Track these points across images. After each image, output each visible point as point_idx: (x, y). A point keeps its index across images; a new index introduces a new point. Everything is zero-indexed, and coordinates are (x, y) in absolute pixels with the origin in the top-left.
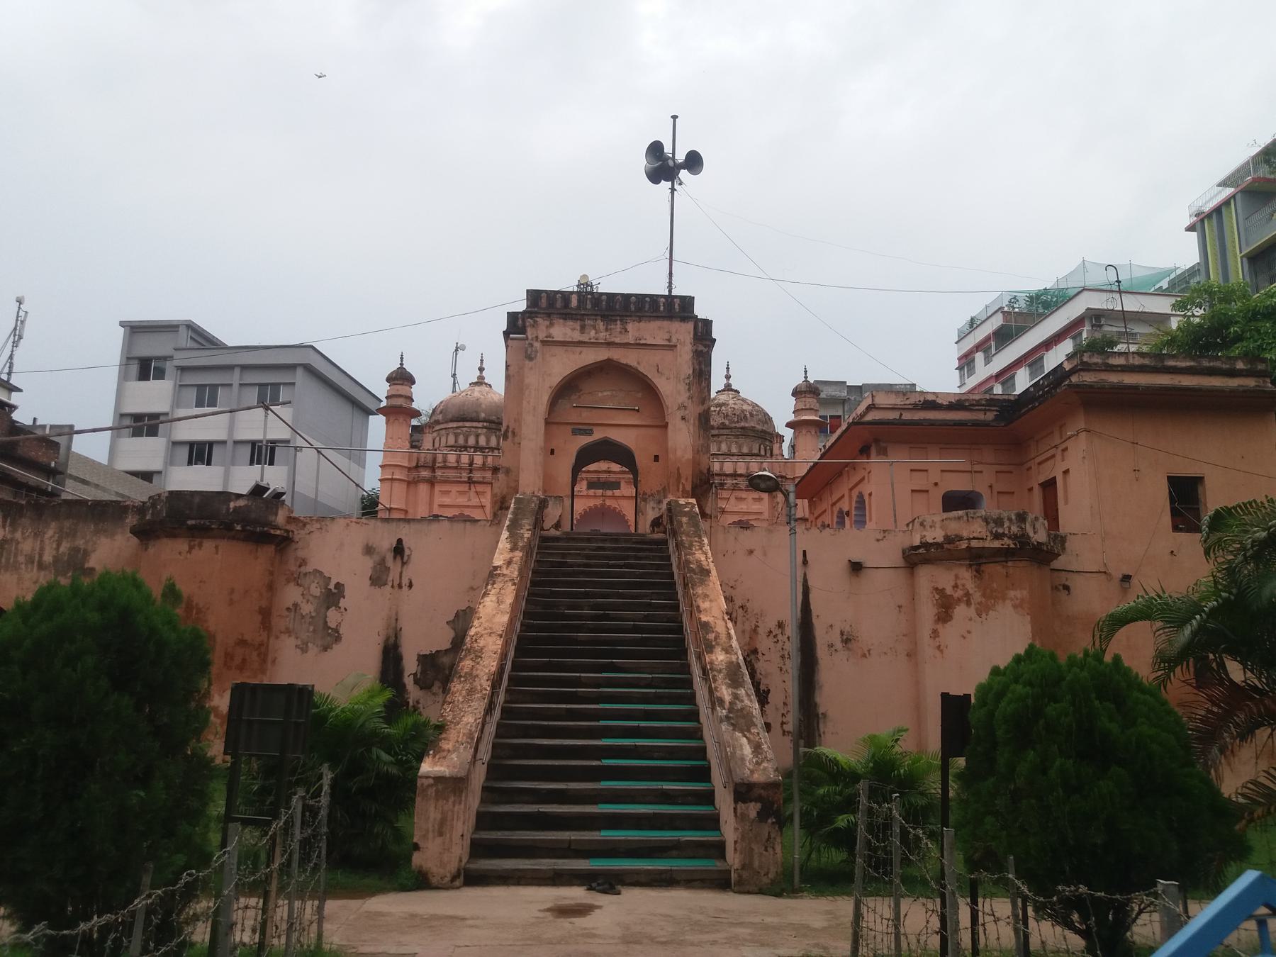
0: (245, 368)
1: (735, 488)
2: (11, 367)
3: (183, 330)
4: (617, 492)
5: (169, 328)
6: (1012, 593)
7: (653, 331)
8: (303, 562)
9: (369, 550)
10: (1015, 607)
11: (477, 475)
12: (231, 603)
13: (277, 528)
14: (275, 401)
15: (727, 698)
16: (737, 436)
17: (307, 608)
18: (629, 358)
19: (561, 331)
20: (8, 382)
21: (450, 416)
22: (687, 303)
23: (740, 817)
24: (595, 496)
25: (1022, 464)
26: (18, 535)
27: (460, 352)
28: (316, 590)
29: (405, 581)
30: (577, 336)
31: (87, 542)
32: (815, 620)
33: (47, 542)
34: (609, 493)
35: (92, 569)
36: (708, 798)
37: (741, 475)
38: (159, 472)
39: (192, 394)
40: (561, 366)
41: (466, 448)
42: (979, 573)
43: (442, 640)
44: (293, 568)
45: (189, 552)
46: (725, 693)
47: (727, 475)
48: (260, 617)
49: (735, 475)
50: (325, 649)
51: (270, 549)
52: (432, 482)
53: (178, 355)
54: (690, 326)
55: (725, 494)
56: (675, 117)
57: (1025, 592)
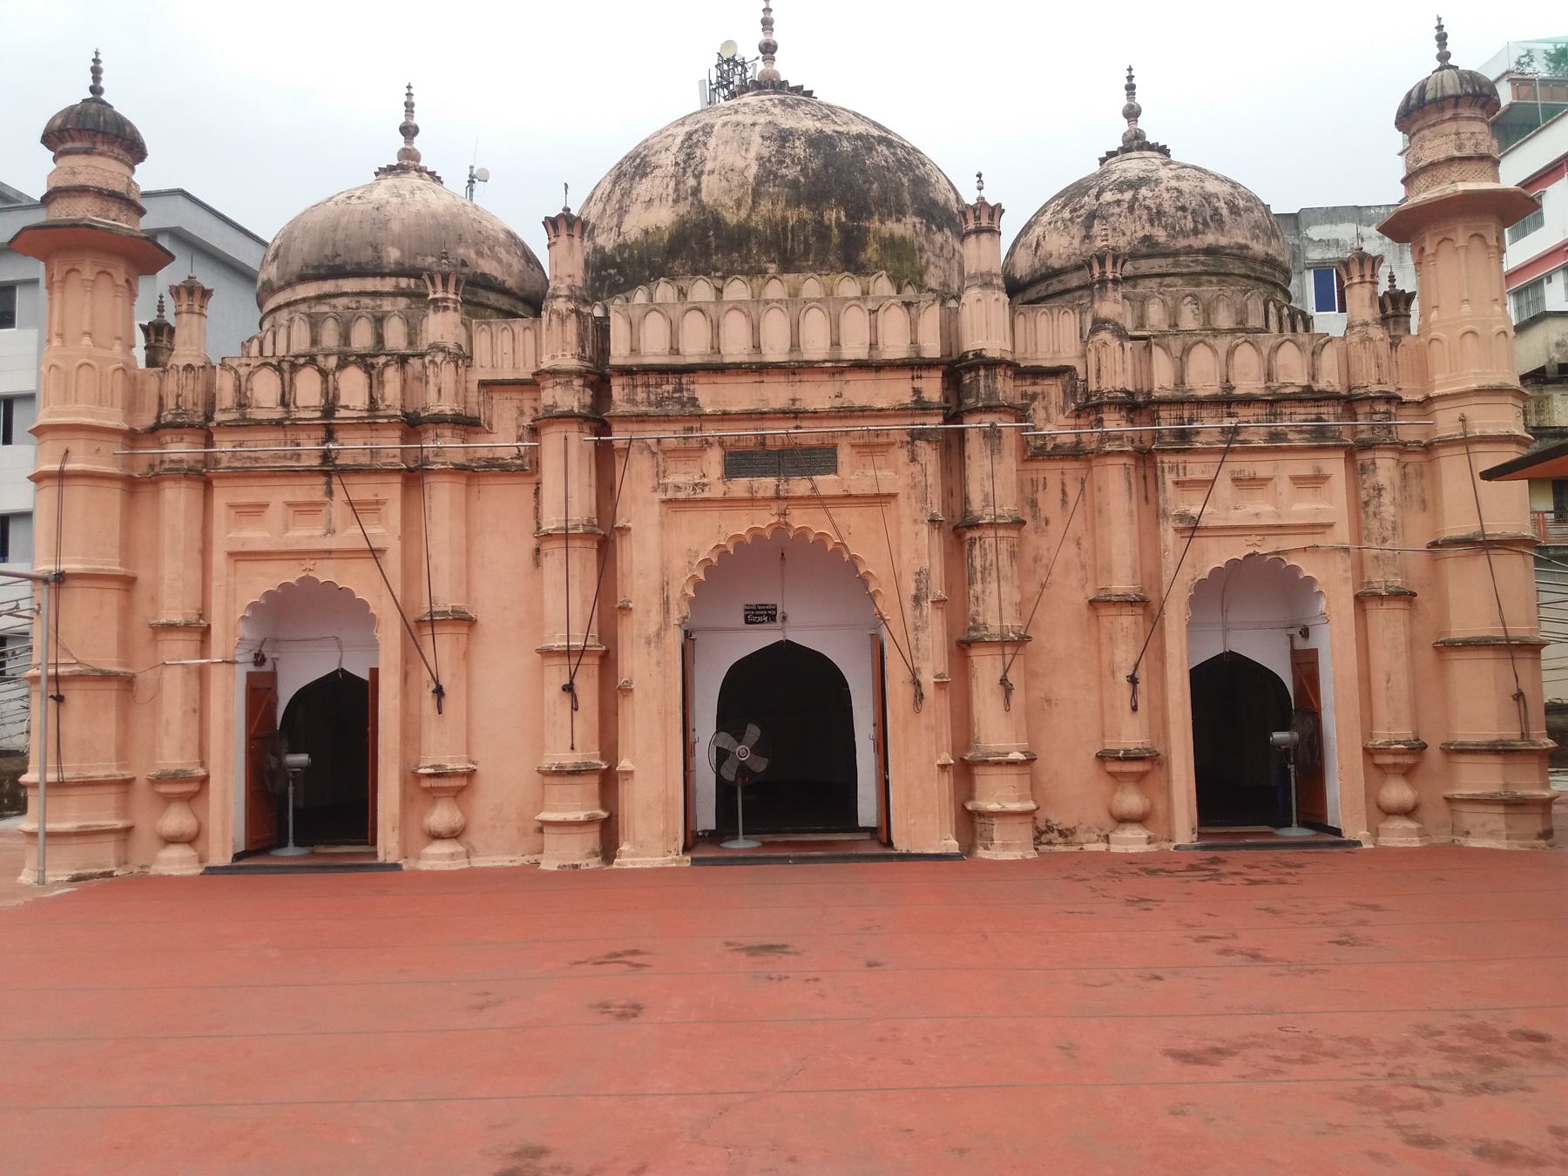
1: (1232, 443)
4: (827, 484)
11: (351, 447)
16: (1194, 277)
21: (295, 266)
24: (752, 501)
27: (478, 185)
34: (800, 486)
37: (1248, 400)
47: (1200, 403)
49: (1226, 401)
52: (202, 477)
55: (1197, 468)
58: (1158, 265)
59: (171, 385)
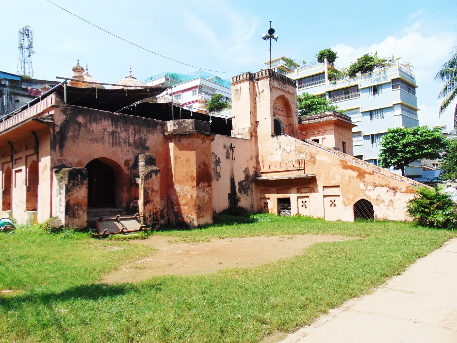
9: (225, 147)
18: (286, 95)
26: (119, 130)
29: (234, 158)
30: (278, 86)
31: (145, 136)
33: (130, 134)
35: (148, 147)
45: (202, 144)
50: (218, 180)
56: (270, 22)
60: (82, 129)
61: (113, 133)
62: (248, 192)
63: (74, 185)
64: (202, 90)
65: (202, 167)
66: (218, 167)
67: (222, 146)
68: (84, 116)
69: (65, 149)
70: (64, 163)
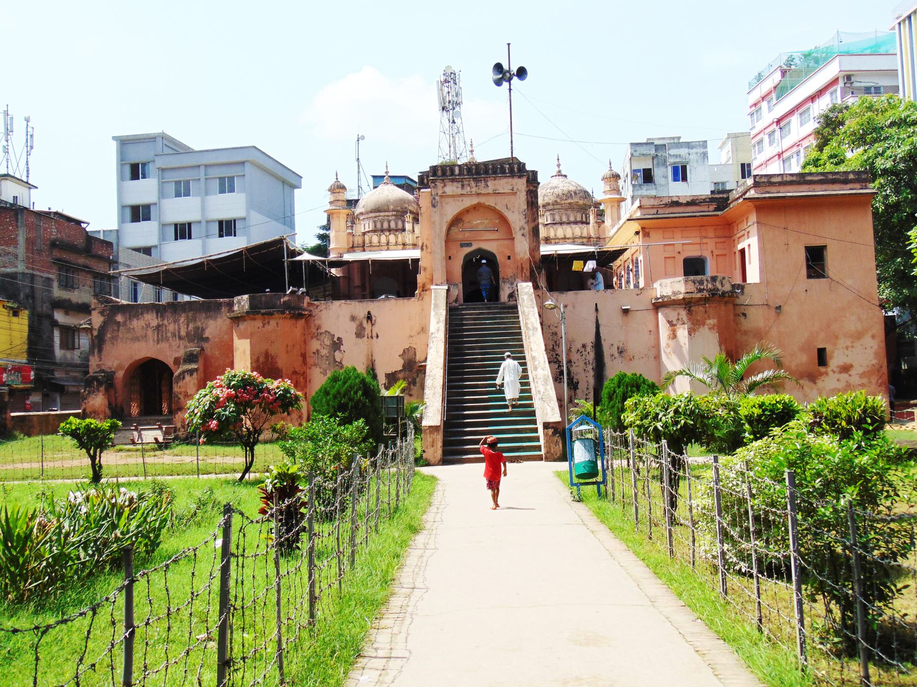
0: (206, 166)
2: (28, 171)
3: (159, 140)
5: (151, 139)
6: (708, 322)
7: (503, 184)
8: (319, 328)
9: (353, 318)
10: (710, 329)
12: (287, 352)
13: (304, 310)
14: (232, 190)
15: (542, 390)
16: (566, 209)
17: (324, 352)
18: (490, 201)
19: (452, 188)
20: (27, 183)
21: (369, 209)
22: (521, 167)
23: (546, 435)
25: (731, 237)
26: (166, 322)
28: (328, 342)
29: (374, 335)
30: (460, 191)
32: (603, 342)
35: (208, 338)
36: (536, 430)
37: (569, 238)
38: (156, 247)
39: (172, 187)
40: (451, 210)
41: (382, 231)
42: (690, 312)
43: (397, 365)
44: (314, 331)
46: (541, 388)
48: (301, 359)
51: (302, 322)
53: (157, 159)
54: (524, 180)
56: (509, 44)
57: (715, 321)
58: (558, 207)
59: (356, 239)
60: (121, 328)
61: (158, 327)
62: (410, 390)
63: (89, 392)
64: (856, 85)
65: (262, 359)
66: (337, 354)
67: (348, 318)
68: (124, 313)
69: (104, 353)
70: (103, 367)
